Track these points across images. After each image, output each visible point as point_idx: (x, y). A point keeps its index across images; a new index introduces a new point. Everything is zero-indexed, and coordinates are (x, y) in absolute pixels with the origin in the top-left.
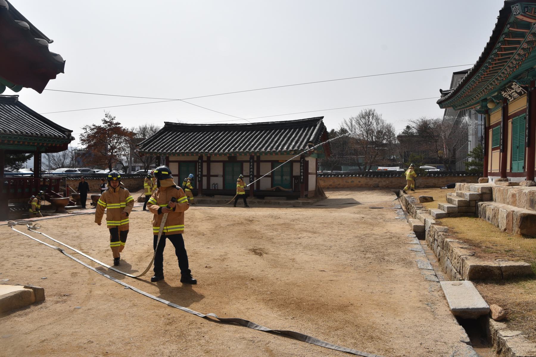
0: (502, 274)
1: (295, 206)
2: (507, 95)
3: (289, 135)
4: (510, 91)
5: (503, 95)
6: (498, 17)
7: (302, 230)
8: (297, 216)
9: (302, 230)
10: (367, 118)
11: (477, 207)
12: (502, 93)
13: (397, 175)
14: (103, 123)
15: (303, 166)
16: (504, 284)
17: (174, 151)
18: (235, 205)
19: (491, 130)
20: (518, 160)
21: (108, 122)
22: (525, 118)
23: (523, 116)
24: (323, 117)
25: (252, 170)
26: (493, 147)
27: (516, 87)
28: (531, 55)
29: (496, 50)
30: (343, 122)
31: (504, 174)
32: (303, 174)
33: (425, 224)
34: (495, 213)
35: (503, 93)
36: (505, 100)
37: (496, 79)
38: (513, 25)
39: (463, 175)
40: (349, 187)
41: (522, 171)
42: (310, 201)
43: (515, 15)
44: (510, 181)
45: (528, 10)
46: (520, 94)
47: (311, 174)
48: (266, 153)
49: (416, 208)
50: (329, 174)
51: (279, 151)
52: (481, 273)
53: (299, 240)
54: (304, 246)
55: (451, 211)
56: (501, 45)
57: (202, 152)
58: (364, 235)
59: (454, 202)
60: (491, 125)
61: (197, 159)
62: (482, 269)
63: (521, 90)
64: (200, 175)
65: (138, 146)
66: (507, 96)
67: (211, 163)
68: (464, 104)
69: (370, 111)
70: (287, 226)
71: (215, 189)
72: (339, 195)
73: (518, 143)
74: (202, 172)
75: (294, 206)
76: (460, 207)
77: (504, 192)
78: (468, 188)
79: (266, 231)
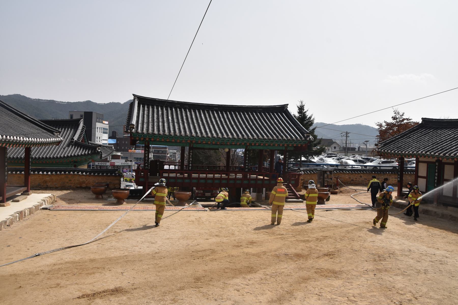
64: (436, 181)
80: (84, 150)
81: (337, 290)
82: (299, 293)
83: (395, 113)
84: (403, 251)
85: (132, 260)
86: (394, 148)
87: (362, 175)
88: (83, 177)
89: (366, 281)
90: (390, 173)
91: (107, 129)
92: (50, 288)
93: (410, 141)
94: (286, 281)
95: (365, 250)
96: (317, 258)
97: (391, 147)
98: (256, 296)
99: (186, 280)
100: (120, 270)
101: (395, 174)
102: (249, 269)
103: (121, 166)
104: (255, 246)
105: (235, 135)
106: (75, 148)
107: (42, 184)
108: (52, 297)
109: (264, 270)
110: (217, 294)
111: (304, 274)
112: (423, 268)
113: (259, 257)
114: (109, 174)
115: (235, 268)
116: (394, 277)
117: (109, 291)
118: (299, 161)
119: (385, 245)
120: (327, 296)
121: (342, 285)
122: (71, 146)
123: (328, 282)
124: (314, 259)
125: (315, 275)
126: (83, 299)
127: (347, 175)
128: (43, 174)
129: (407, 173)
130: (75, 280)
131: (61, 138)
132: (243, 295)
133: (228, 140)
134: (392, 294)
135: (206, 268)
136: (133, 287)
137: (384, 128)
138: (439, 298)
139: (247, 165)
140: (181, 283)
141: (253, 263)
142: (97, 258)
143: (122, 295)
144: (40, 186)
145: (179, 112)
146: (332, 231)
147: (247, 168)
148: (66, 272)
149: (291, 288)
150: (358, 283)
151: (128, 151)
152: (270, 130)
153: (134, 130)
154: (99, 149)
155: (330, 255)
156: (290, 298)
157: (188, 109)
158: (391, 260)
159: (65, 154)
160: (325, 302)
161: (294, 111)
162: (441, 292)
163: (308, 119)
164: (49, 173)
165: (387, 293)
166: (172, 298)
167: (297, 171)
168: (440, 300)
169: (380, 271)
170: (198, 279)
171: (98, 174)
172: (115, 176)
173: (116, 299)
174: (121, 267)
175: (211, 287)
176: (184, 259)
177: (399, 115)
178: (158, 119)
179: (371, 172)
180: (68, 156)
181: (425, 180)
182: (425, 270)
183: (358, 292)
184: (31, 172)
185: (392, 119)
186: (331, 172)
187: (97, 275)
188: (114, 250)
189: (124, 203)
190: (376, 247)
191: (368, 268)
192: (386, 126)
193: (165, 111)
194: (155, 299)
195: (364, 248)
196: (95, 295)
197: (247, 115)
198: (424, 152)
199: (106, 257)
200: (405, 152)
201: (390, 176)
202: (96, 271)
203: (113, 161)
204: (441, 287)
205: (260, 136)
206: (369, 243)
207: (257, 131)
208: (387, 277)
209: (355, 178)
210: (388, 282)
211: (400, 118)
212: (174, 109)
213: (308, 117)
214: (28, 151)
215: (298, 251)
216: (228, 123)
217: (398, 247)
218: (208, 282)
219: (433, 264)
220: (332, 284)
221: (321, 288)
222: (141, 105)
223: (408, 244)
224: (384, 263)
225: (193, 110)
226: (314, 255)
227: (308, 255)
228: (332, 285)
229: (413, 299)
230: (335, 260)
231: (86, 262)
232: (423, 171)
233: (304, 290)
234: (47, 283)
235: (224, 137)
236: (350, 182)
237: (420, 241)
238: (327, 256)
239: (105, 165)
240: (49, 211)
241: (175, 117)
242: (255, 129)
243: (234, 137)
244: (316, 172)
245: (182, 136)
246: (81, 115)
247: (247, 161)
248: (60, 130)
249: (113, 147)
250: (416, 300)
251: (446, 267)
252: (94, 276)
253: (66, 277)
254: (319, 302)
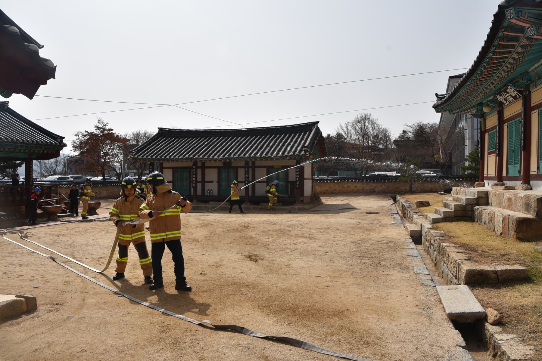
0: (498, 278)
1: (291, 212)
2: (502, 99)
3: (284, 140)
4: (506, 95)
5: (499, 99)
6: (492, 20)
7: (298, 236)
8: (293, 222)
9: (298, 236)
10: (363, 122)
11: (473, 211)
12: (497, 97)
13: (394, 180)
14: (96, 129)
15: (299, 171)
16: (499, 288)
17: (168, 157)
18: (230, 211)
19: (487, 134)
20: (514, 164)
21: (101, 128)
22: (520, 122)
23: (519, 120)
24: (318, 122)
25: (247, 176)
26: (489, 151)
27: (512, 91)
28: (526, 59)
29: (491, 54)
30: (339, 127)
31: (500, 178)
32: (299, 179)
33: (421, 228)
34: (491, 217)
35: (498, 97)
36: (501, 104)
37: (491, 83)
38: (508, 28)
39: (459, 179)
40: (346, 192)
41: (518, 175)
42: (306, 206)
43: (509, 19)
44: (506, 185)
45: (521, 14)
46: (515, 98)
47: (307, 179)
48: (261, 158)
49: (412, 213)
50: (325, 180)
51: (275, 156)
52: (477, 277)
53: (295, 245)
54: (299, 252)
55: (447, 216)
56: (496, 49)
57: (196, 158)
58: (360, 240)
59: (451, 207)
60: (487, 129)
61: (191, 165)
62: (477, 273)
63: (517, 93)
65: (132, 152)
66: (502, 100)
67: (206, 169)
68: (459, 108)
69: (366, 115)
70: (283, 232)
71: (210, 196)
72: (335, 200)
73: (514, 147)
74: (196, 178)
75: (290, 212)
76: (455, 212)
77: (500, 196)
78: (464, 192)
79: (262, 238)
127: (63, 190)
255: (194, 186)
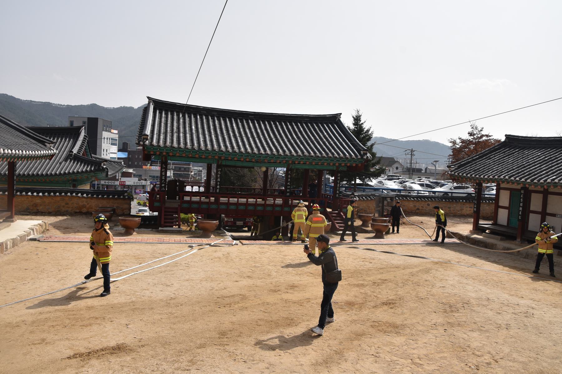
64: (520, 212)
80: (86, 166)
81: (398, 349)
82: (350, 353)
83: (472, 128)
84: (480, 300)
85: (141, 307)
86: (471, 171)
87: (429, 203)
88: (84, 199)
89: (434, 338)
90: (464, 201)
91: (116, 140)
92: (33, 344)
93: (490, 163)
94: (334, 338)
95: (433, 297)
96: (374, 307)
97: (467, 169)
98: (296, 357)
99: (207, 335)
100: (124, 321)
101: (470, 202)
102: (289, 321)
103: (133, 185)
104: (297, 291)
105: (274, 150)
106: (74, 163)
107: (32, 208)
108: (34, 357)
109: (307, 323)
110: (247, 354)
111: (358, 328)
112: (505, 322)
113: (301, 305)
114: (116, 197)
115: (271, 319)
116: (469, 333)
117: (109, 349)
118: (353, 184)
119: (457, 291)
120: (386, 357)
121: (405, 343)
122: (69, 160)
123: (387, 339)
124: (370, 309)
125: (371, 330)
126: (75, 360)
127: (411, 203)
128: (33, 195)
129: (484, 202)
130: (65, 334)
131: (55, 151)
132: (280, 355)
133: (266, 157)
134: (466, 356)
135: (234, 319)
136: (140, 344)
137: (458, 146)
138: (524, 360)
139: (289, 189)
140: (201, 338)
141: (294, 313)
142: (96, 304)
143: (125, 354)
144: (28, 211)
145: (205, 121)
146: (392, 272)
147: (288, 192)
148: (54, 324)
149: (341, 347)
150: (425, 341)
151: (142, 168)
152: (318, 146)
153: (147, 141)
154: (104, 165)
155: (390, 303)
156: (340, 359)
157: (217, 117)
158: (465, 311)
159: (61, 171)
160: (383, 365)
161: (348, 122)
162: (527, 353)
163: (366, 132)
164: (41, 194)
165: (461, 354)
166: (189, 358)
167: (350, 197)
168: (525, 364)
169: (451, 325)
170: (223, 334)
171: (103, 196)
172: (124, 198)
173: (118, 359)
174: (126, 317)
175: (240, 345)
176: (206, 306)
177: (477, 131)
178: (178, 128)
179: (442, 200)
180: (65, 173)
181: (507, 211)
182: (507, 324)
183: (425, 352)
184: (16, 192)
185: (468, 135)
186: (392, 198)
187: (95, 327)
188: (117, 295)
189: (134, 233)
190: (446, 294)
191: (437, 321)
192: (461, 144)
193: (187, 119)
194: (168, 360)
195: (432, 295)
196: (90, 355)
197: (289, 126)
198: (507, 177)
199: (107, 303)
200: (484, 176)
201: (464, 204)
202: (93, 322)
203: (123, 179)
204: (526, 347)
205: (306, 152)
206: (438, 288)
207: (302, 146)
208: (460, 334)
209: (422, 207)
210: (462, 340)
211: (478, 133)
212: (198, 117)
213: (365, 130)
214: (12, 166)
215: (350, 298)
216: (266, 135)
217: (473, 295)
218: (236, 338)
219: (517, 316)
220: (392, 341)
221: (378, 347)
222: (158, 111)
223: (486, 291)
224: (456, 315)
225: (223, 117)
226: (370, 303)
227: (362, 303)
228: (392, 342)
229: (493, 362)
230: (396, 311)
231: (81, 310)
232: (504, 200)
233: (357, 349)
234: (30, 337)
235: (260, 152)
236: (414, 212)
237: (501, 287)
238: (386, 305)
239: (113, 184)
240: (38, 242)
241: (199, 126)
242: (299, 143)
243: (273, 153)
244: (373, 198)
245: (208, 150)
246: (83, 121)
247: (288, 184)
248: (55, 141)
249: (123, 163)
250: (495, 363)
251: (532, 321)
252: (90, 329)
253: (55, 330)
254: (376, 365)
255: (520, 218)
